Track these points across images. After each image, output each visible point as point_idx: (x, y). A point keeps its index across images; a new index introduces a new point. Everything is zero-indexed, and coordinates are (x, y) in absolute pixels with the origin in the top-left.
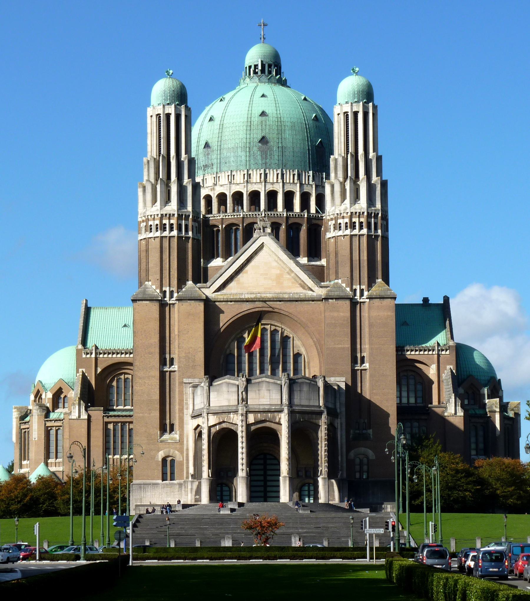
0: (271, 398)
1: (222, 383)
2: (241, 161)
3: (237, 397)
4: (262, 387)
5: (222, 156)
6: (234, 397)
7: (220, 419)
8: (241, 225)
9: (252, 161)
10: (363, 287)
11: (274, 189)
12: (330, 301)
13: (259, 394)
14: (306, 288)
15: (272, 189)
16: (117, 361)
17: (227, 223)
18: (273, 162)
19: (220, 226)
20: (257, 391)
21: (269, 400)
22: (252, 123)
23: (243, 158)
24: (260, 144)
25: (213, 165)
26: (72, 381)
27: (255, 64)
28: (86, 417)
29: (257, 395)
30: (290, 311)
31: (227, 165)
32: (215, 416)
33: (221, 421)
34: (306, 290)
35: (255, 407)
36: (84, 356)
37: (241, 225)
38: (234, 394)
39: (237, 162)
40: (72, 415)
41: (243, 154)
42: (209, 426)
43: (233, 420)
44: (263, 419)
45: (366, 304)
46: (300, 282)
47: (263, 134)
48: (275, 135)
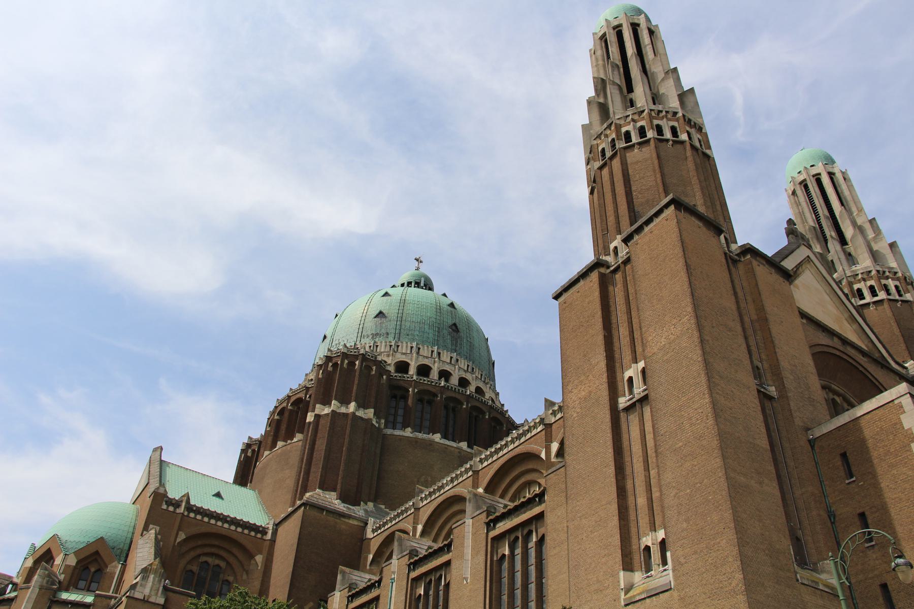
2: (429, 338)
5: (403, 327)
8: (439, 395)
9: (441, 342)
11: (467, 378)
15: (464, 376)
16: (214, 531)
17: (421, 387)
18: (462, 352)
19: (410, 390)
22: (442, 308)
23: (431, 335)
24: (451, 330)
25: (388, 334)
26: (121, 546)
27: (417, 281)
28: (161, 601)
31: (410, 337)
36: (164, 507)
37: (439, 395)
39: (423, 338)
40: (137, 590)
41: (431, 331)
46: (866, 343)
47: (453, 322)
48: (464, 328)
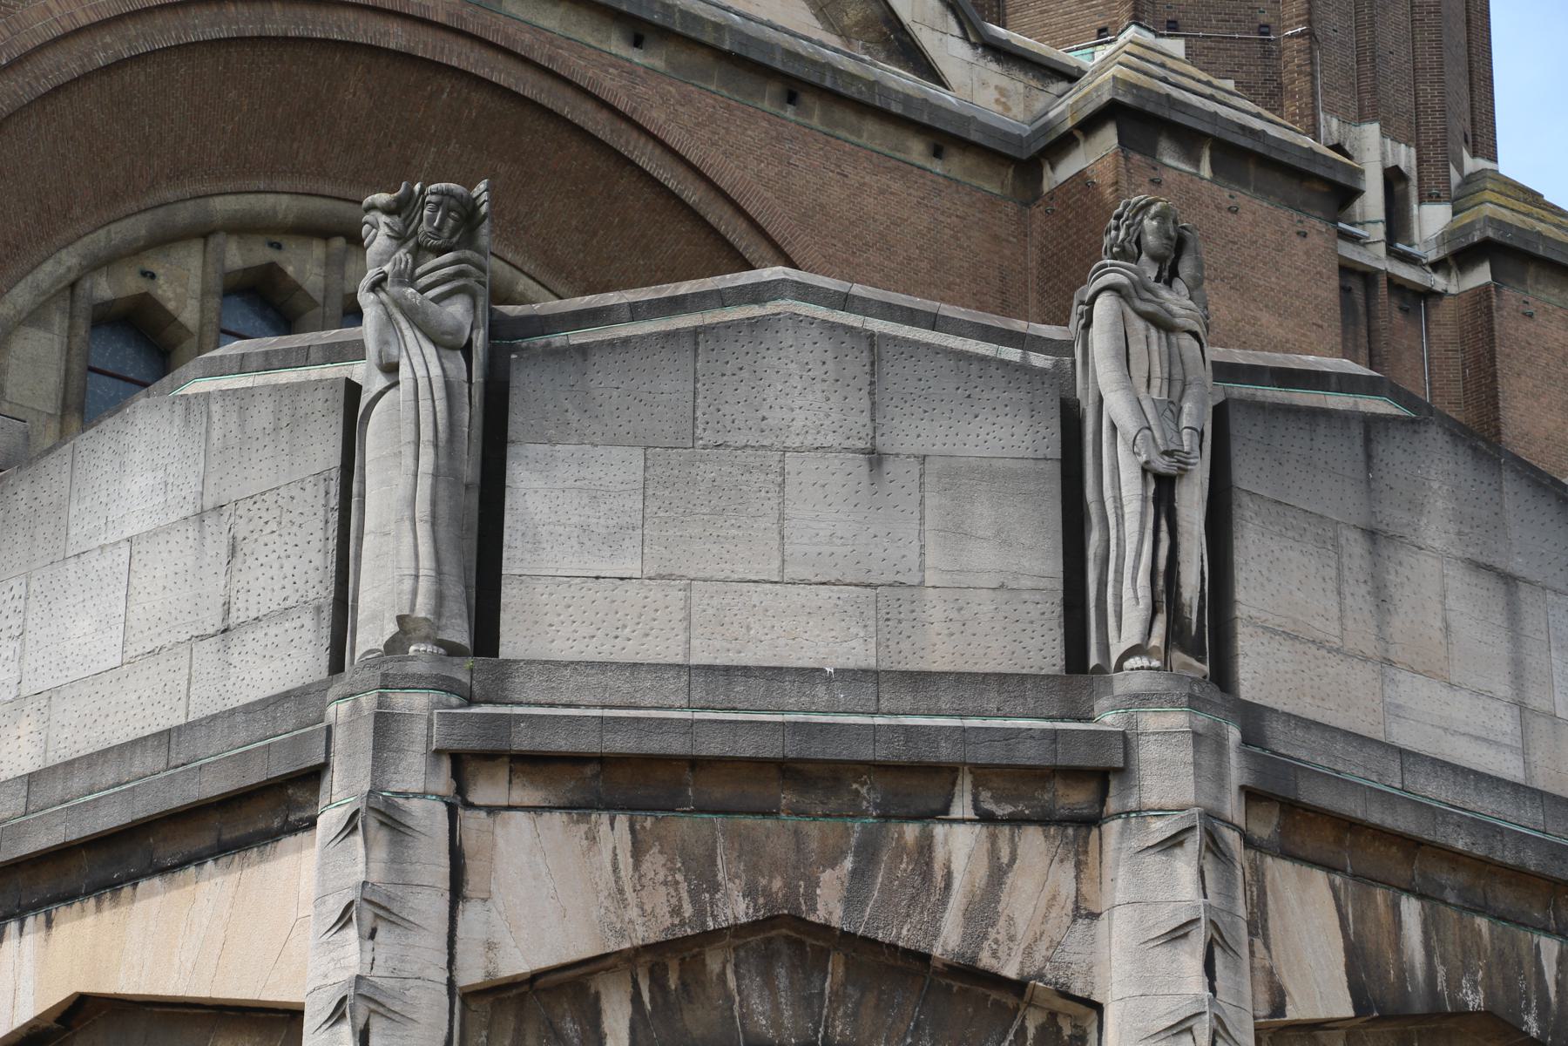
0: (1535, 700)
1: (754, 323)
3: (1052, 566)
4: (1416, 506)
6: (985, 558)
7: (705, 882)
10: (1405, 157)
12: (1170, 157)
13: (1381, 598)
14: (852, 15)
20: (1355, 546)
21: (1505, 723)
29: (1359, 597)
30: (729, 175)
32: (614, 832)
33: (736, 908)
34: (843, 34)
35: (1355, 767)
38: (983, 514)
42: (471, 974)
43: (984, 910)
44: (1475, 1000)
45: (1445, 314)
